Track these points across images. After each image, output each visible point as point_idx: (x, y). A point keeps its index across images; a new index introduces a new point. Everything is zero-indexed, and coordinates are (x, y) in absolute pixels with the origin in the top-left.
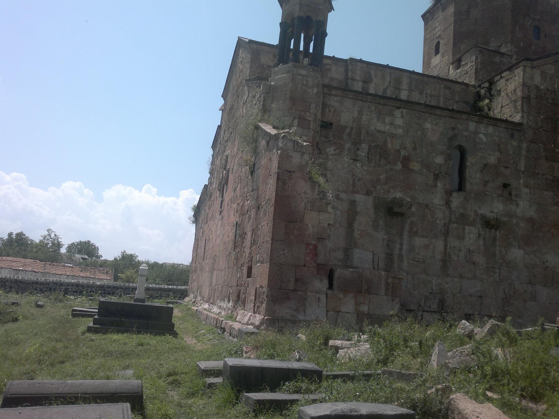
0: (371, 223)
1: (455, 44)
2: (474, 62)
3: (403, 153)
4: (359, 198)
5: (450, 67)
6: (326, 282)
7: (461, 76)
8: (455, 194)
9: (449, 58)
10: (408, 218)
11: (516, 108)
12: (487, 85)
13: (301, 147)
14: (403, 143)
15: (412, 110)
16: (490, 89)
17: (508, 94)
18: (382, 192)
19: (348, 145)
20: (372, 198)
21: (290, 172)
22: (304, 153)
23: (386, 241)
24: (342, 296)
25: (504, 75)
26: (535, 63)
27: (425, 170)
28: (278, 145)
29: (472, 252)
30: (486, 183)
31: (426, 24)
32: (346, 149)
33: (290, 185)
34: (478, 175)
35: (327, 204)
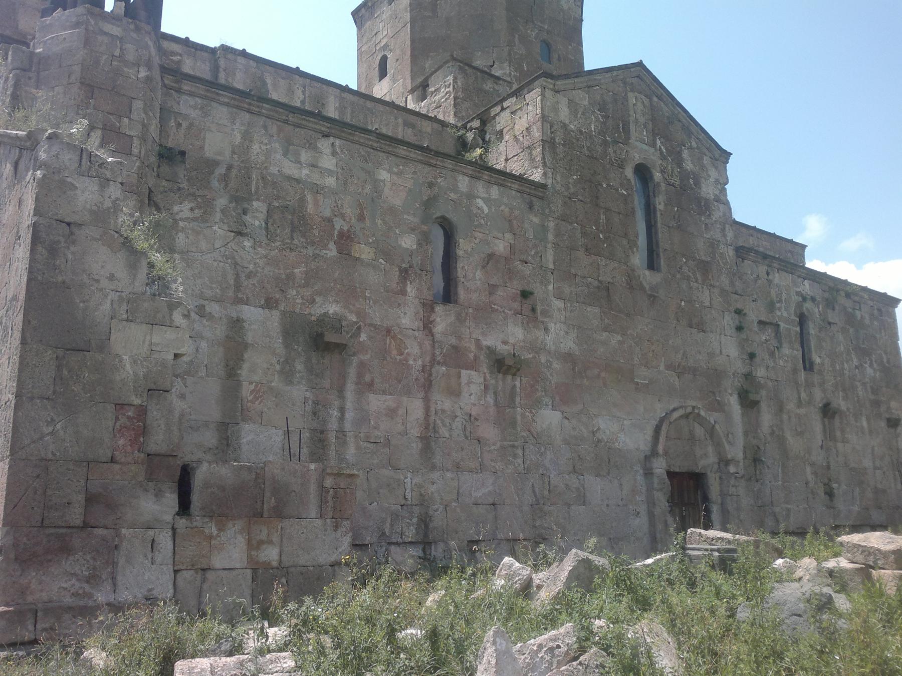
0: (278, 367)
1: (414, 58)
2: (451, 86)
3: (339, 224)
4: (251, 313)
6: (171, 500)
8: (439, 309)
10: (354, 354)
11: (532, 159)
12: (476, 124)
13: (100, 165)
14: (337, 206)
15: (352, 141)
16: (482, 132)
17: (515, 137)
19: (222, 202)
20: (278, 314)
21: (69, 224)
22: (108, 180)
23: (310, 402)
24: (214, 531)
25: (505, 104)
26: (559, 83)
27: (381, 260)
28: (36, 159)
29: (476, 419)
30: (492, 289)
32: (218, 210)
33: (70, 256)
34: (479, 274)
35: (172, 307)
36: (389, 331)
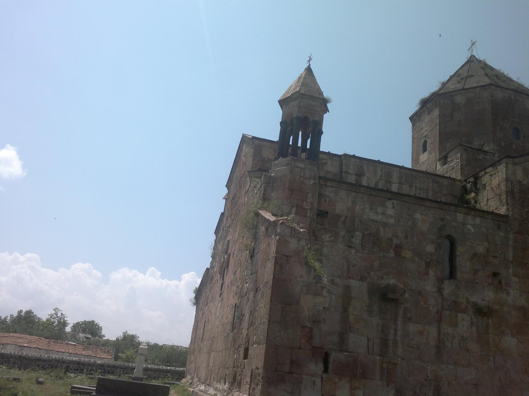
0: (366, 308)
1: (440, 142)
2: (459, 159)
3: (395, 241)
4: (354, 283)
5: (437, 163)
6: (321, 366)
7: (447, 171)
8: (446, 282)
9: (435, 155)
12: (472, 180)
13: (298, 233)
15: (402, 201)
16: (475, 184)
18: (376, 278)
19: (342, 233)
21: (287, 256)
22: (301, 239)
23: (381, 325)
25: (487, 170)
26: (516, 160)
28: (276, 231)
30: (476, 272)
31: (413, 125)
33: (287, 269)
35: (323, 288)
36: (420, 293)
